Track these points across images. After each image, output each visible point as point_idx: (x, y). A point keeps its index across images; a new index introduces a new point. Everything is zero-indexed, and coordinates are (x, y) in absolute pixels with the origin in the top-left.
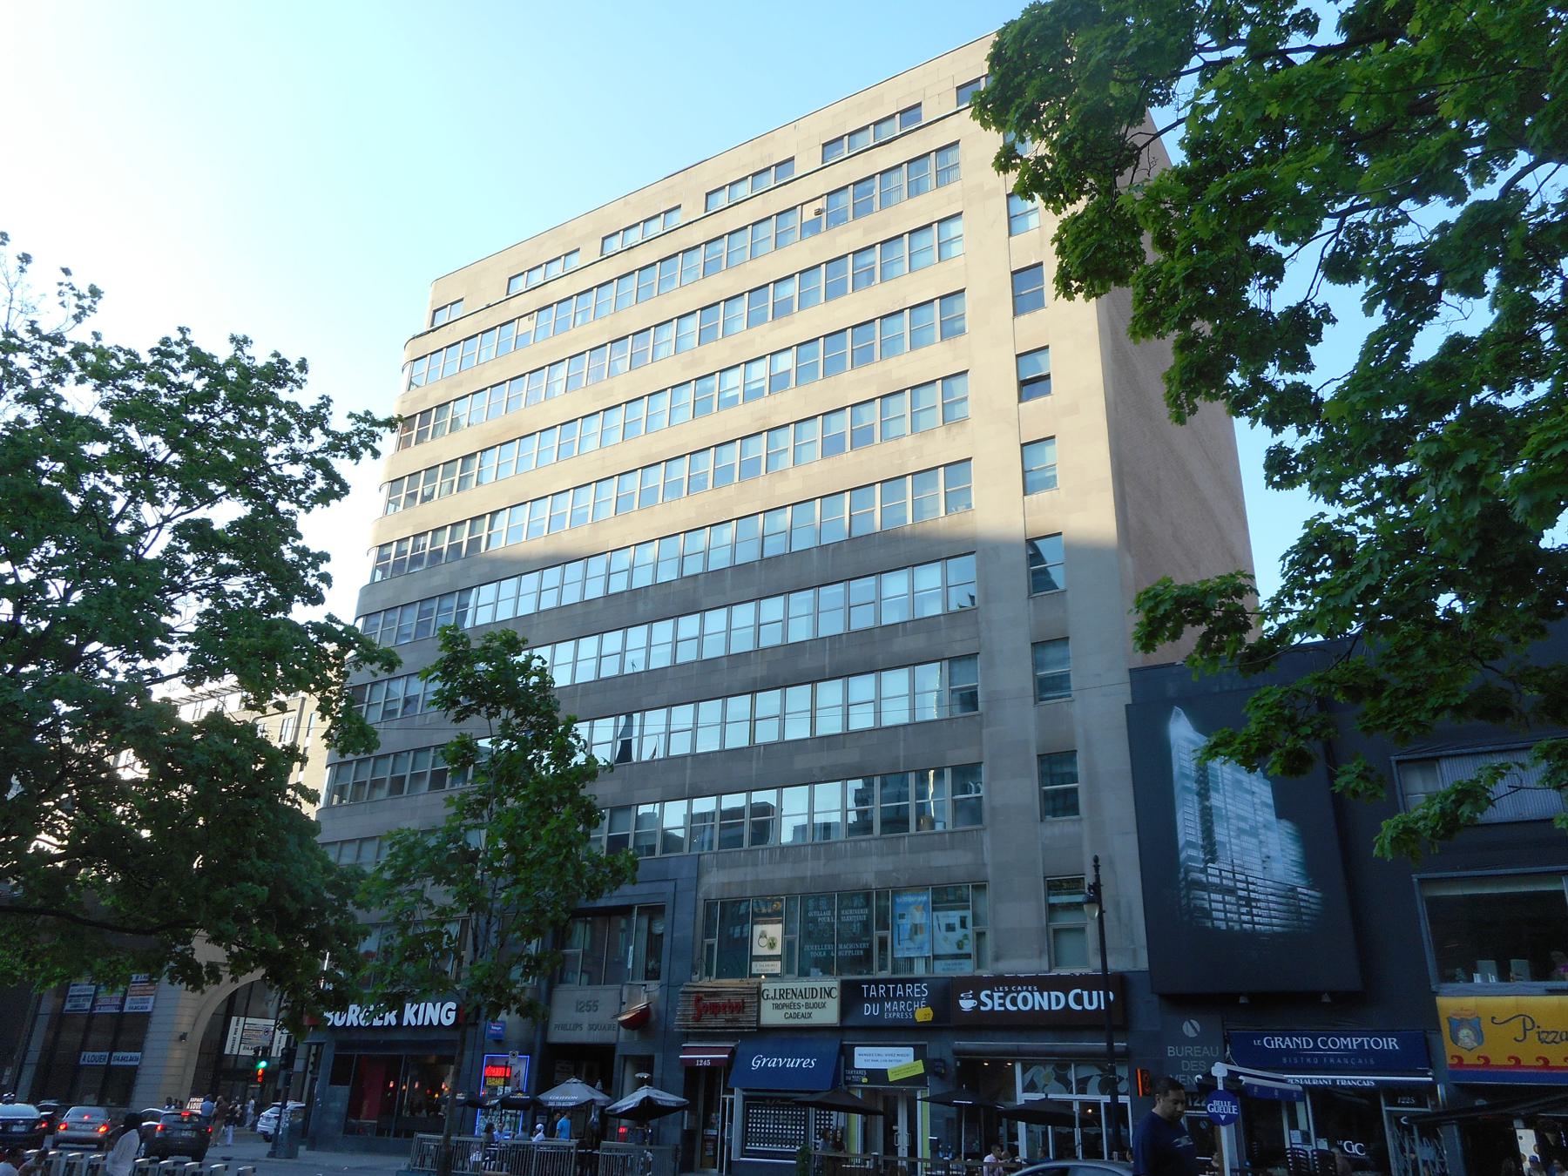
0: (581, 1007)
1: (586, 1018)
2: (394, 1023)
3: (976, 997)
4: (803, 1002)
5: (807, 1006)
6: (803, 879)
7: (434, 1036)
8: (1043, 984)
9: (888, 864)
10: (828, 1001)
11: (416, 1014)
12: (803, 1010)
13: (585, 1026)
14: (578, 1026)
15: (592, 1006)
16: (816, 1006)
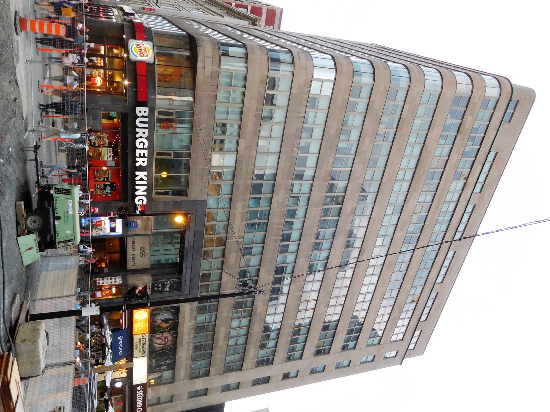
0: (142, 249)
1: (137, 252)
2: (137, 165)
3: (141, 390)
4: (141, 347)
5: (140, 348)
6: (183, 336)
7: (130, 185)
8: (144, 403)
9: (184, 358)
10: (141, 354)
11: (141, 180)
12: (138, 347)
13: (134, 253)
14: (134, 249)
15: (142, 255)
16: (140, 351)
